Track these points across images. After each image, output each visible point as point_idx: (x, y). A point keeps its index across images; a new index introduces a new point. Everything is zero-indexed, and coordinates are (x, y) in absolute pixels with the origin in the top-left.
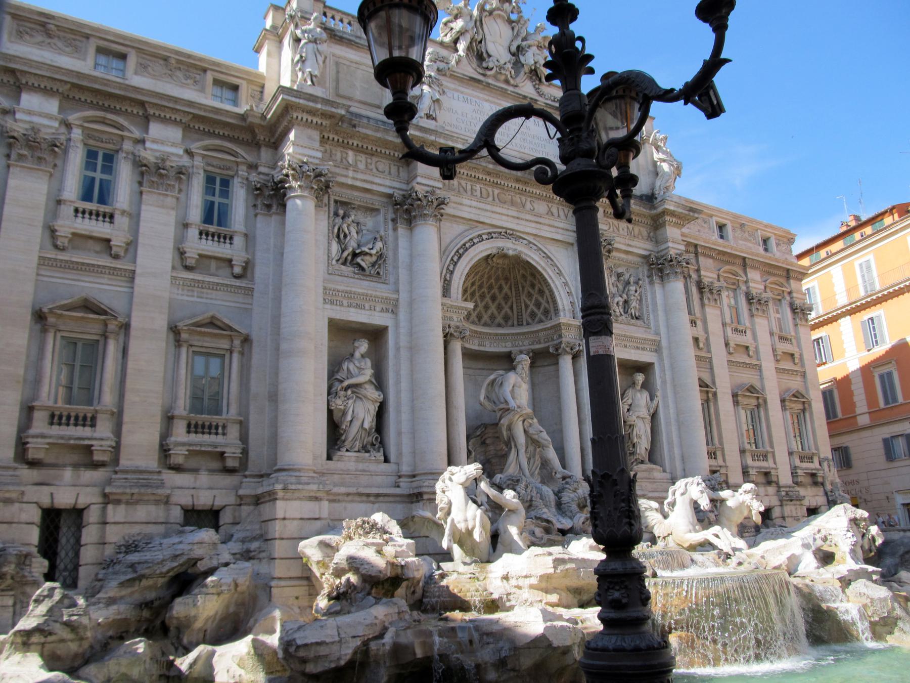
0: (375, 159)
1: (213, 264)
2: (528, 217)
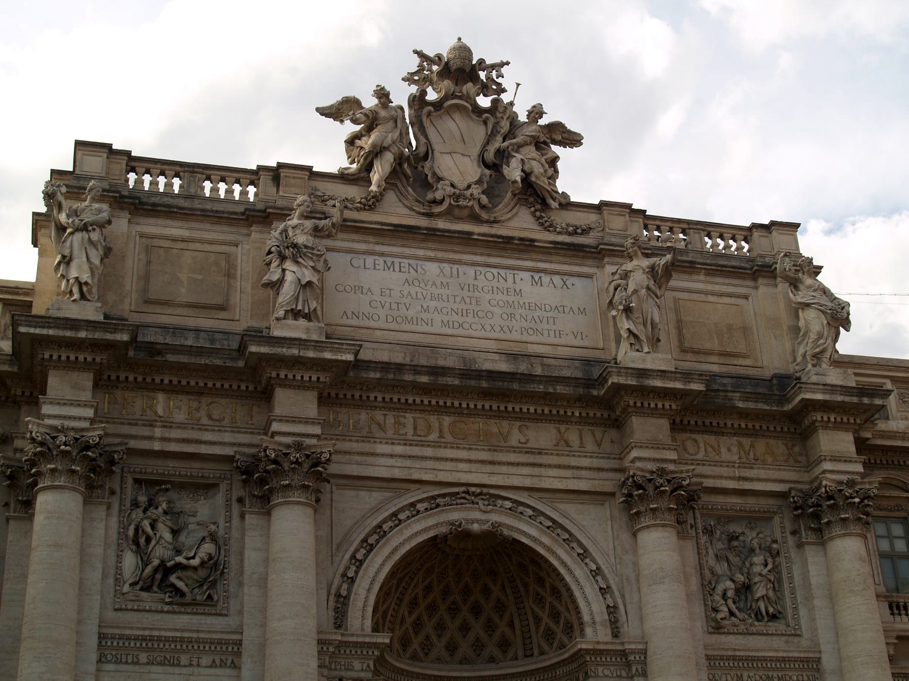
0: (205, 400)
2: (512, 457)
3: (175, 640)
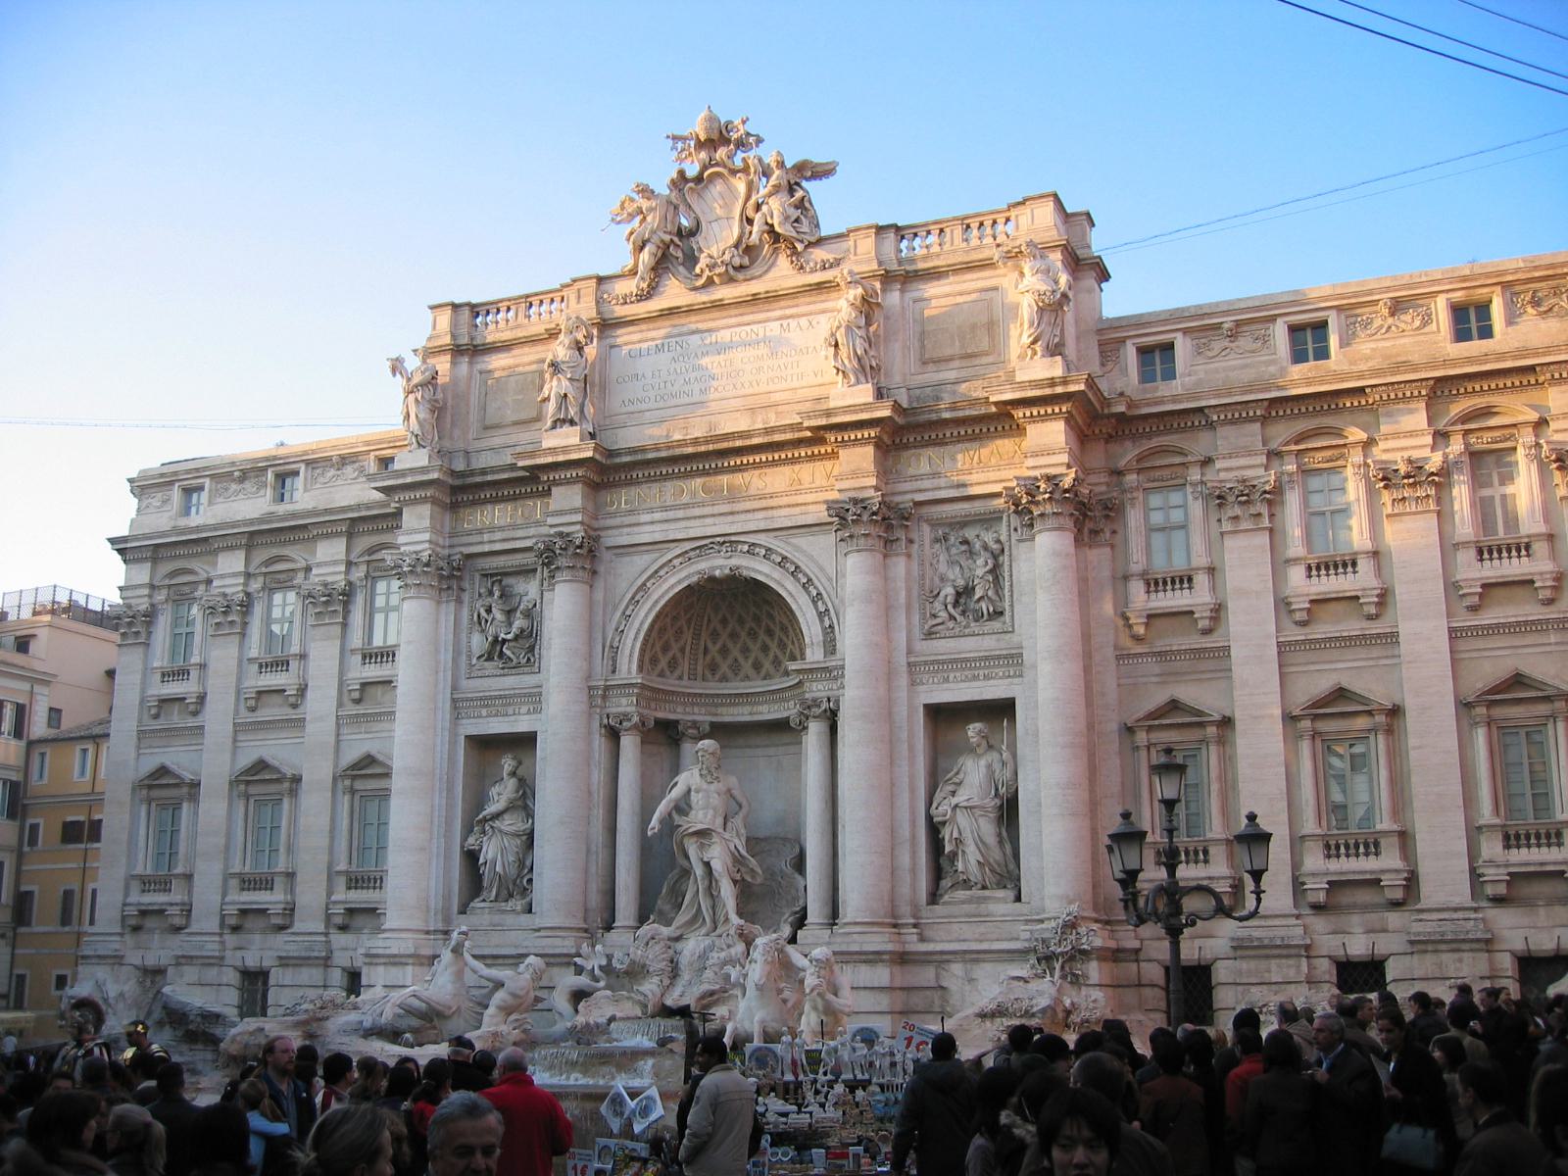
0: (519, 503)
1: (379, 690)
3: (500, 697)
